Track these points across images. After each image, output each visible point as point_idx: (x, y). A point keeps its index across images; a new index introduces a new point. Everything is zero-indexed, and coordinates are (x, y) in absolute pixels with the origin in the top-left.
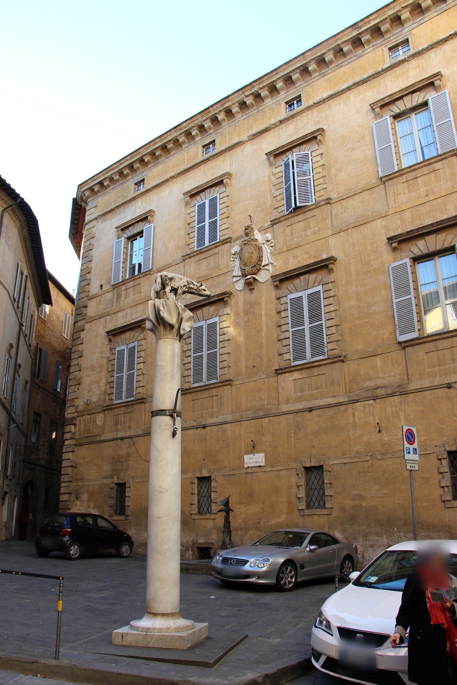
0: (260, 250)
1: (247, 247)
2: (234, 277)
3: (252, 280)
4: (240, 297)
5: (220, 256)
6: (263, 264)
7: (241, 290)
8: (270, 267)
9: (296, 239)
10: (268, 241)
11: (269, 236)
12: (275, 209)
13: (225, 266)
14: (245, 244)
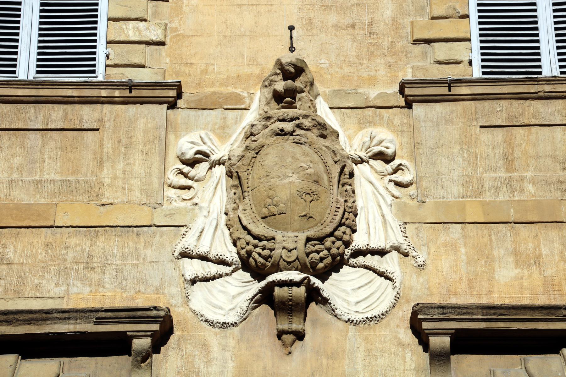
0: (346, 176)
1: (287, 144)
2: (184, 255)
3: (301, 292)
4: (216, 352)
5: (108, 147)
6: (360, 240)
7: (224, 325)
8: (390, 263)
9: (531, 188)
10: (381, 156)
11: (387, 138)
12: (416, 42)
13: (137, 195)
14: (282, 133)
